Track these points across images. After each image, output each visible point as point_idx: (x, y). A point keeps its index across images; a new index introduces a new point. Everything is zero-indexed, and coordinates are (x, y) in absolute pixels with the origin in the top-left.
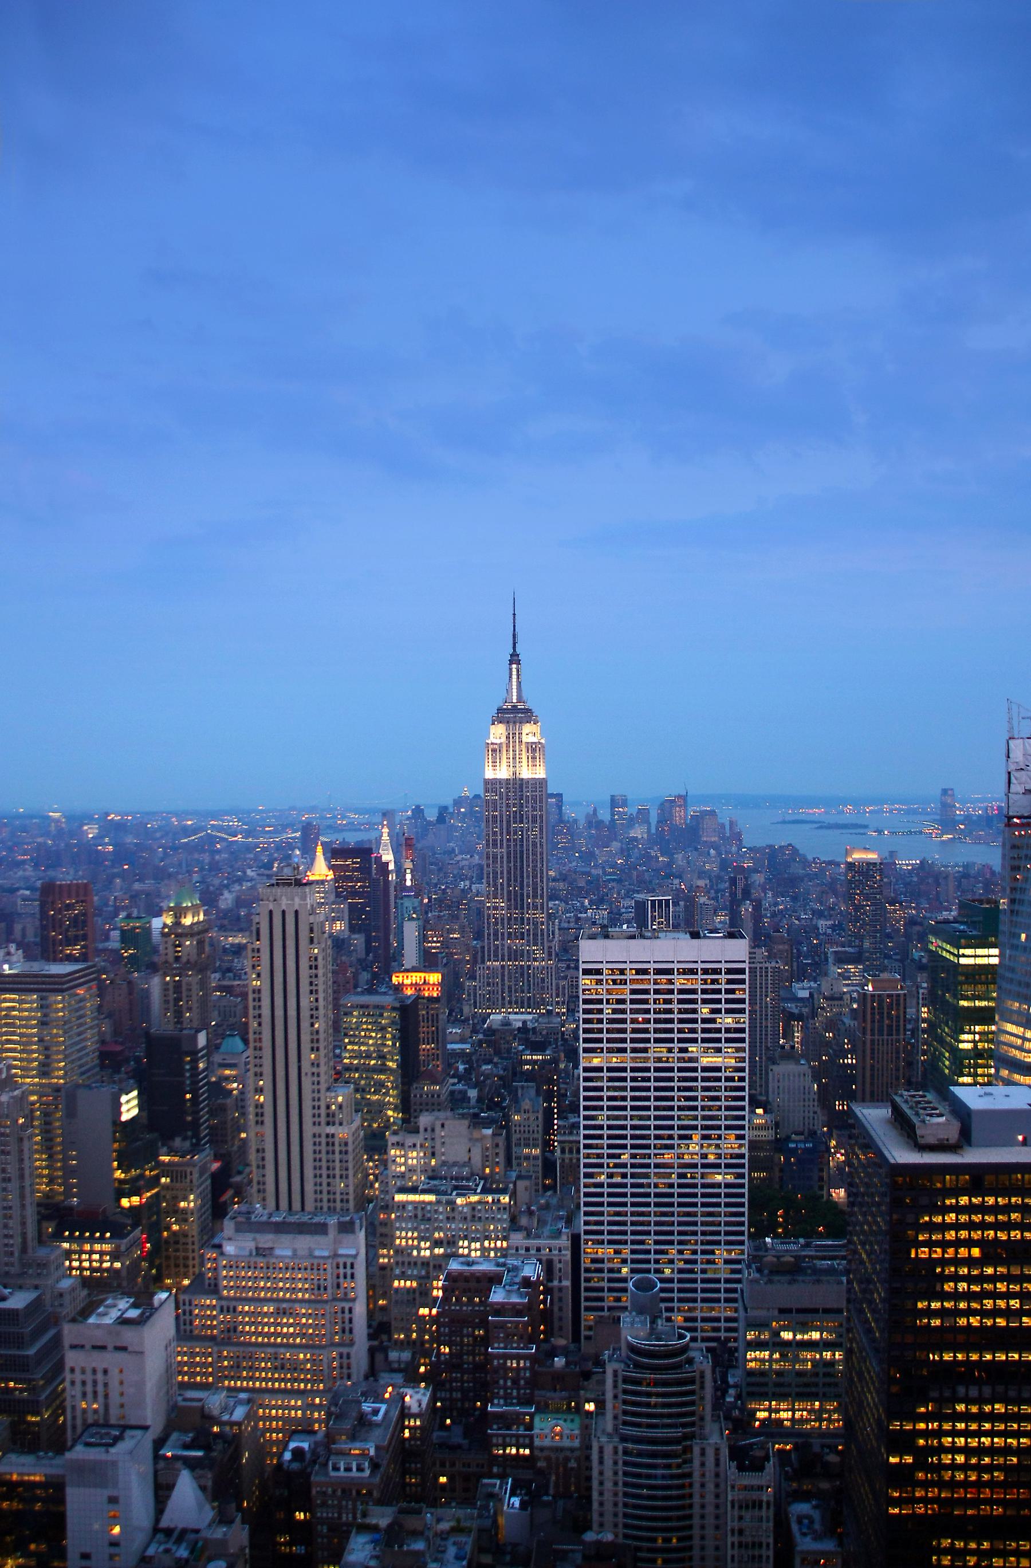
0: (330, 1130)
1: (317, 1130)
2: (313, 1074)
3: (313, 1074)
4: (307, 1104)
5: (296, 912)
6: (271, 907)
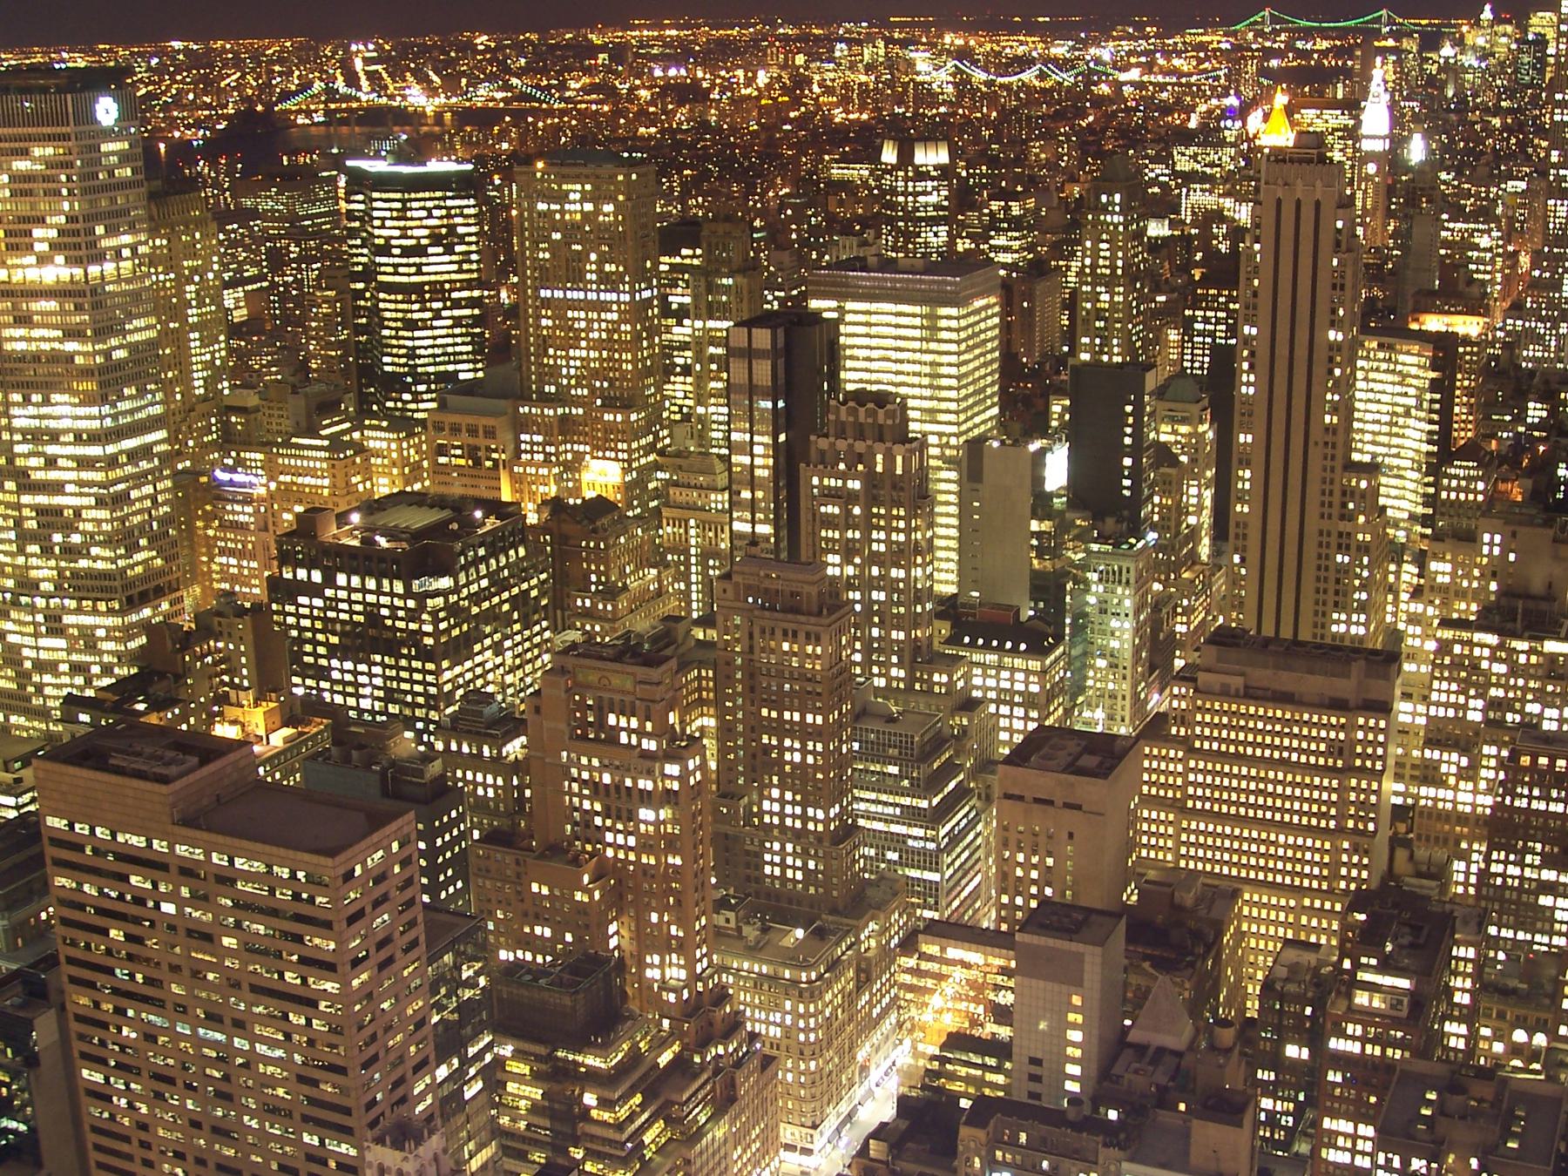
0: (1344, 526)
1: (1325, 525)
2: (1326, 443)
3: (1326, 443)
4: (1314, 489)
5: (1318, 204)
6: (1280, 194)
